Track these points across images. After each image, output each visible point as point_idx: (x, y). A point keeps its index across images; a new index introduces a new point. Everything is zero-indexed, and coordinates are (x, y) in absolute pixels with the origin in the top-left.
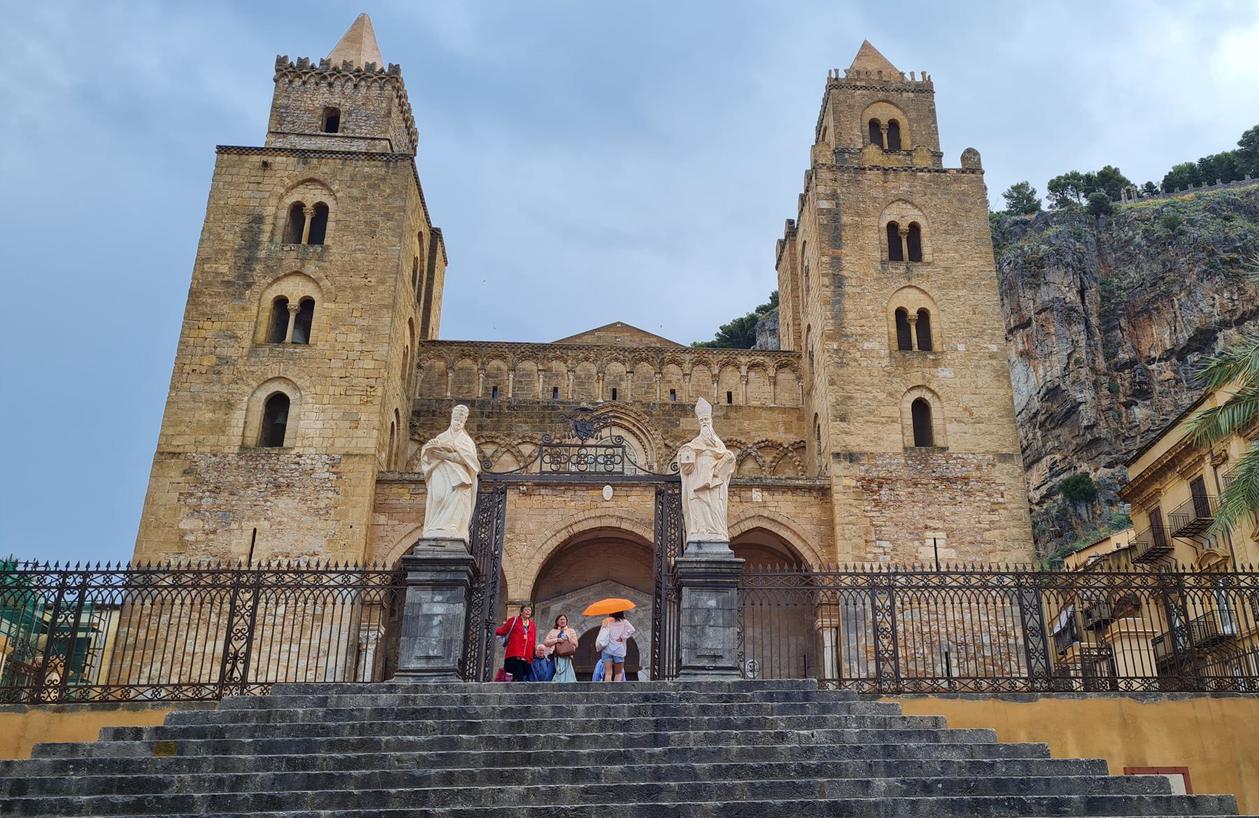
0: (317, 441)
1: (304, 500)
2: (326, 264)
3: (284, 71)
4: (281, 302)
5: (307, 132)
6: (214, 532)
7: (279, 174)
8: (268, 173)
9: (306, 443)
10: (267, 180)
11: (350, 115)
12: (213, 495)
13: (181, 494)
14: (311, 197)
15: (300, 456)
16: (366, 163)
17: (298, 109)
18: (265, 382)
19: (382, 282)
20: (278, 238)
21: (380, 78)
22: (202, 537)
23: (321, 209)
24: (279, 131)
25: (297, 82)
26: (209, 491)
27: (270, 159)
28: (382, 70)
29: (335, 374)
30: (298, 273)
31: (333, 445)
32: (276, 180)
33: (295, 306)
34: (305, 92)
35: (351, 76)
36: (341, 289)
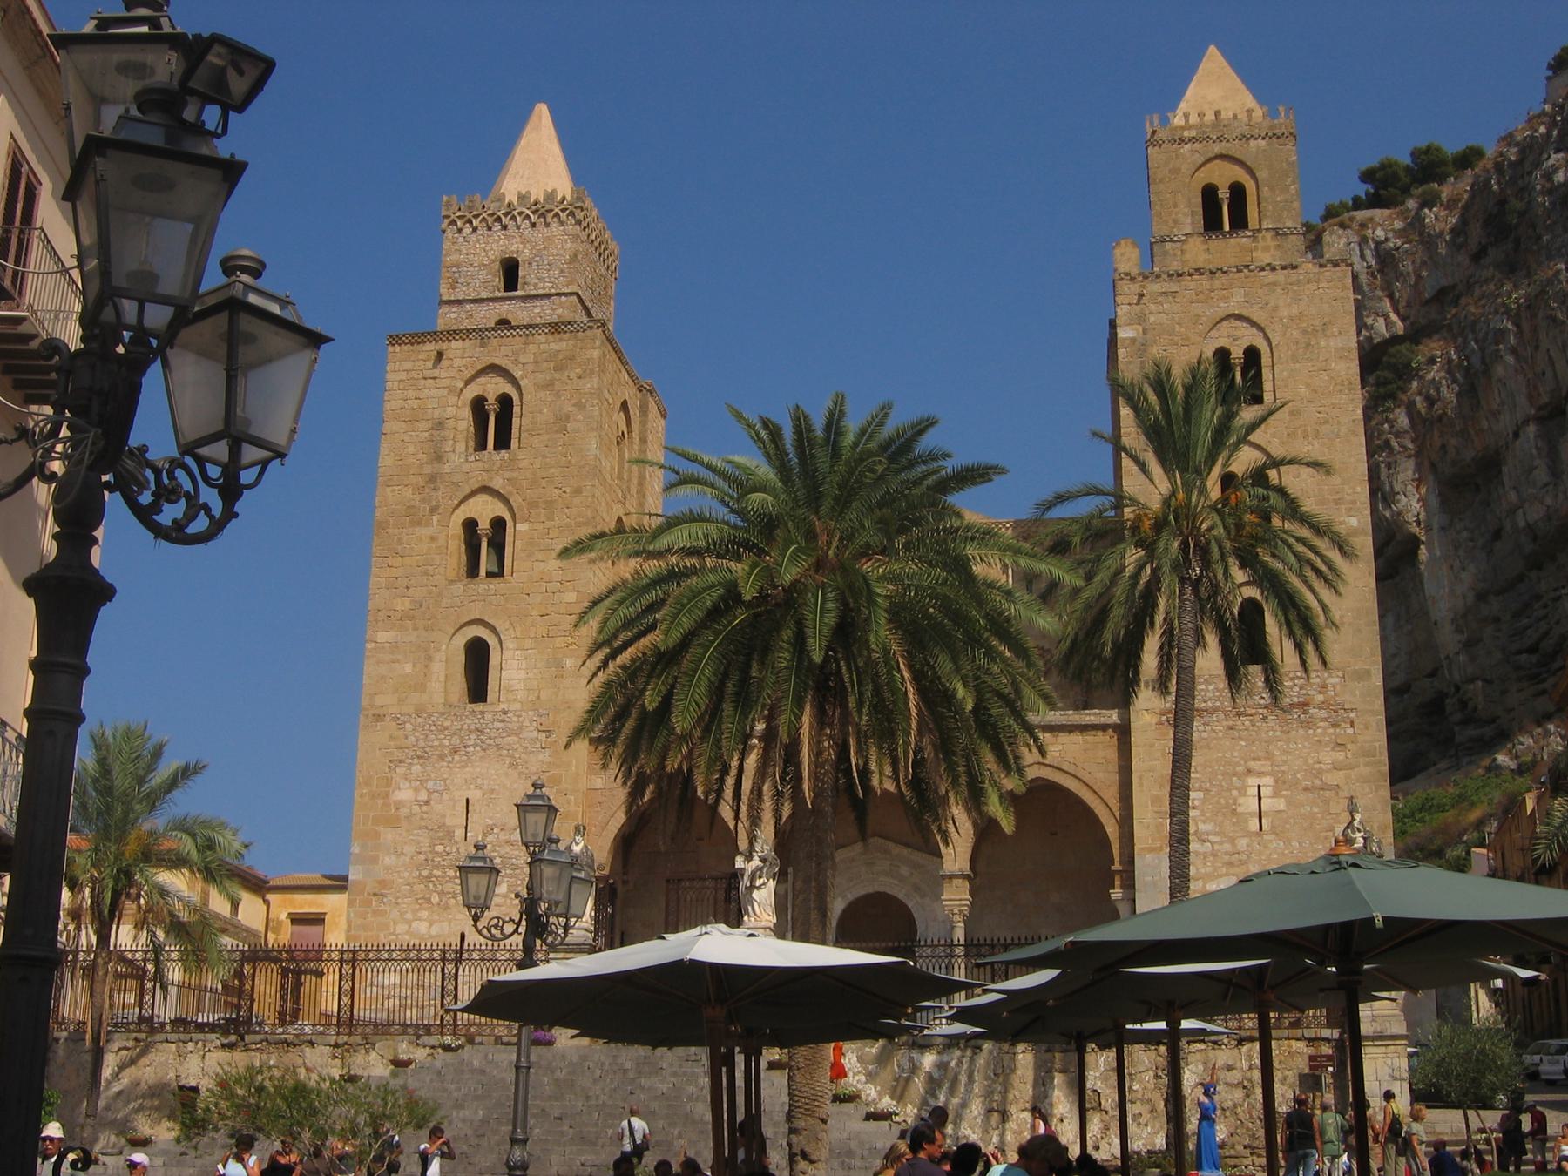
0: (520, 695)
1: (513, 765)
2: (515, 474)
3: (453, 216)
4: (470, 525)
5: (484, 295)
6: (427, 803)
7: (458, 362)
8: (444, 363)
9: (511, 696)
10: (444, 374)
11: (530, 264)
12: (422, 761)
13: (390, 761)
14: (493, 387)
15: (505, 713)
16: (551, 338)
17: (471, 265)
18: (462, 626)
19: (578, 491)
20: (461, 447)
21: (563, 210)
22: (416, 809)
23: (505, 402)
24: (452, 298)
25: (467, 230)
26: (419, 757)
27: (445, 346)
28: (564, 199)
29: (534, 613)
30: (485, 489)
31: (539, 698)
32: (453, 372)
33: (486, 530)
34: (478, 241)
35: (528, 212)
36: (533, 505)
